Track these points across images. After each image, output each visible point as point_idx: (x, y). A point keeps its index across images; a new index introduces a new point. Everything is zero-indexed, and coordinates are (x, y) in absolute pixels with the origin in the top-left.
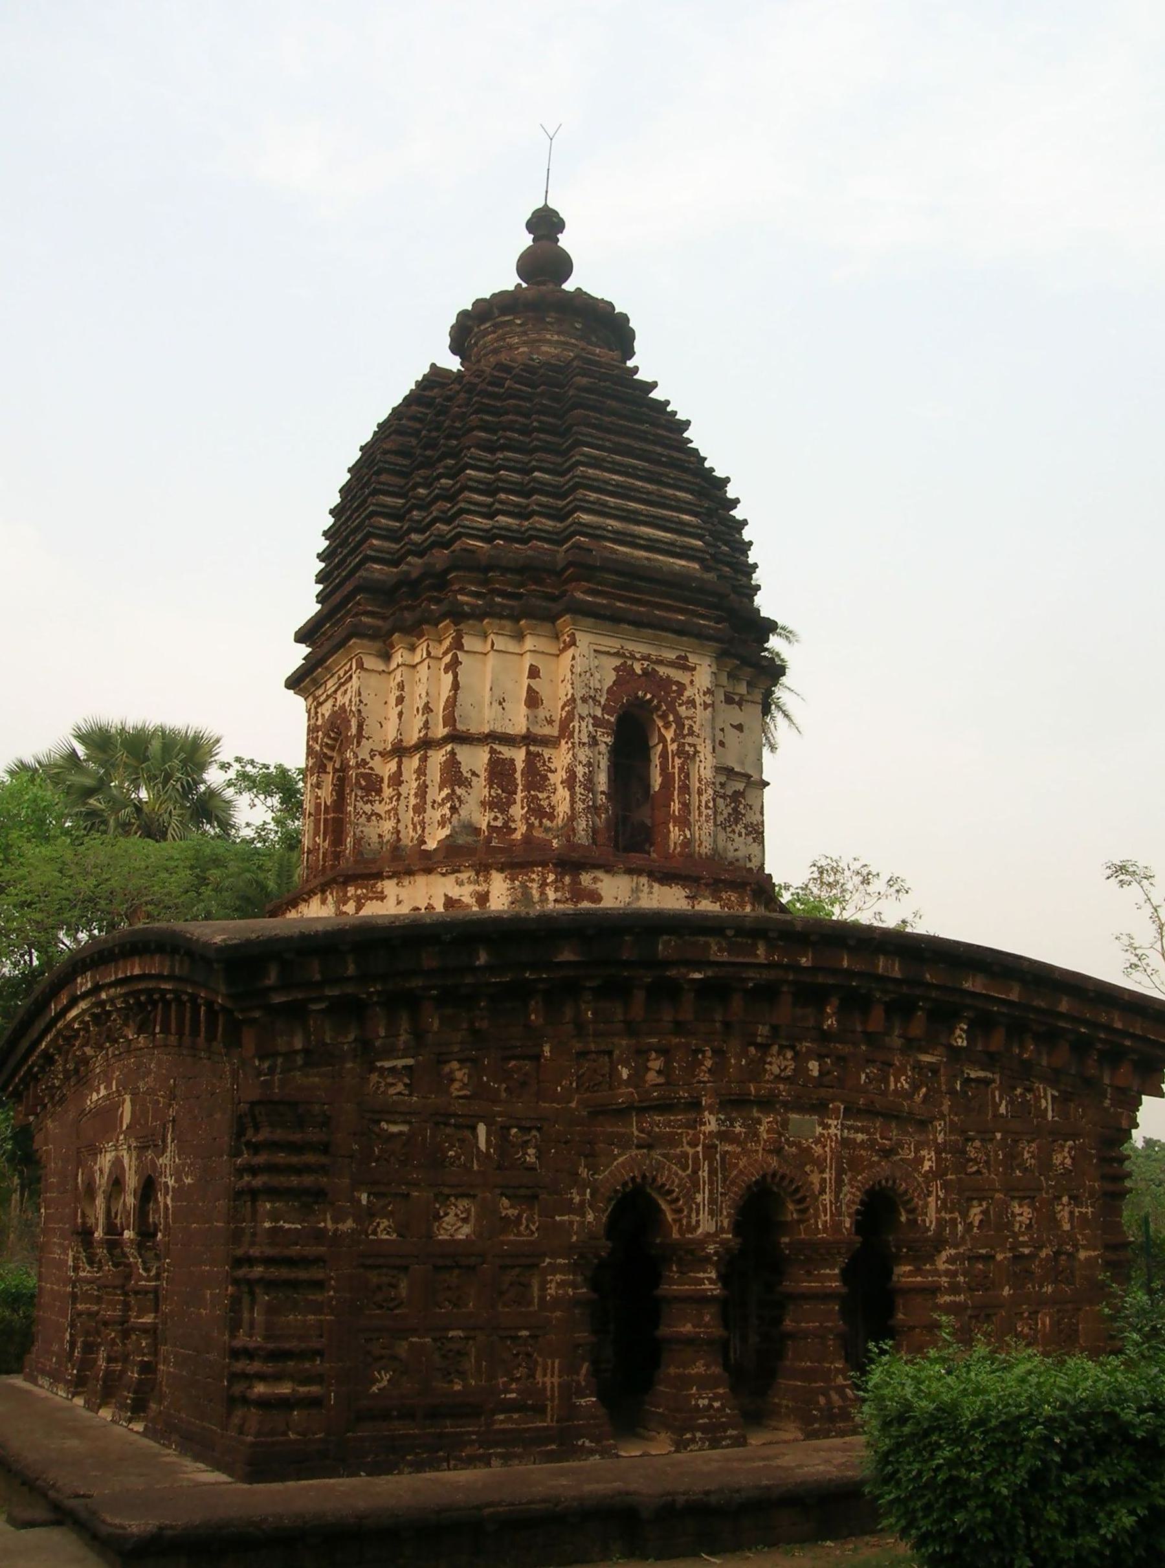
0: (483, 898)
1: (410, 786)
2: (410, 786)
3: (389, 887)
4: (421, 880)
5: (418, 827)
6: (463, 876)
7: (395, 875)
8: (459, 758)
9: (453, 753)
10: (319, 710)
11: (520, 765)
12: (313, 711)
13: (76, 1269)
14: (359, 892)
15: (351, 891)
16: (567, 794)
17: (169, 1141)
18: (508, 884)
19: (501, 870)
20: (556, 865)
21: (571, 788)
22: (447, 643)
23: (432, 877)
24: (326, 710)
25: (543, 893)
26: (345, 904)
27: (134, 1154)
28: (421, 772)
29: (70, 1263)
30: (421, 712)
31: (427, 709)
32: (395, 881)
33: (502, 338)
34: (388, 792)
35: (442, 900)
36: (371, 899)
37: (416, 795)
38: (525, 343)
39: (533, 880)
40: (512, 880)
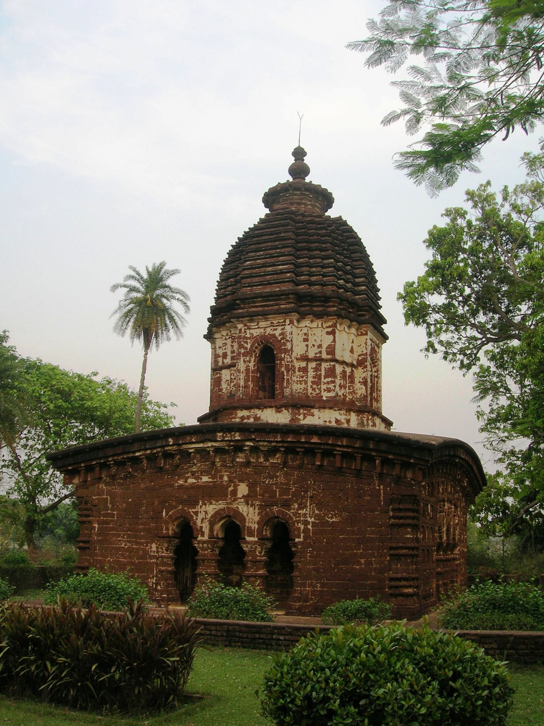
0: (348, 421)
1: (311, 373)
2: (311, 373)
3: (315, 411)
4: (327, 411)
5: (317, 390)
6: (342, 412)
7: (319, 408)
8: (336, 368)
9: (334, 366)
10: (248, 331)
11: (348, 374)
12: (243, 330)
13: (158, 552)
14: (305, 412)
15: (302, 411)
16: (364, 388)
17: (308, 504)
18: (356, 417)
19: (354, 412)
20: (372, 413)
21: (366, 385)
22: (330, 324)
23: (331, 410)
24: (256, 332)
25: (367, 422)
26: (299, 415)
27: (257, 508)
28: (317, 369)
29: (154, 549)
30: (316, 347)
31: (320, 346)
32: (318, 410)
33: (302, 199)
34: (297, 373)
35: (335, 419)
36: (309, 415)
37: (314, 377)
38: (311, 205)
39: (364, 417)
40: (358, 416)
